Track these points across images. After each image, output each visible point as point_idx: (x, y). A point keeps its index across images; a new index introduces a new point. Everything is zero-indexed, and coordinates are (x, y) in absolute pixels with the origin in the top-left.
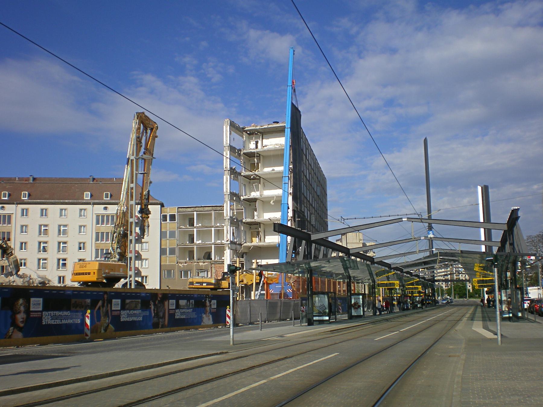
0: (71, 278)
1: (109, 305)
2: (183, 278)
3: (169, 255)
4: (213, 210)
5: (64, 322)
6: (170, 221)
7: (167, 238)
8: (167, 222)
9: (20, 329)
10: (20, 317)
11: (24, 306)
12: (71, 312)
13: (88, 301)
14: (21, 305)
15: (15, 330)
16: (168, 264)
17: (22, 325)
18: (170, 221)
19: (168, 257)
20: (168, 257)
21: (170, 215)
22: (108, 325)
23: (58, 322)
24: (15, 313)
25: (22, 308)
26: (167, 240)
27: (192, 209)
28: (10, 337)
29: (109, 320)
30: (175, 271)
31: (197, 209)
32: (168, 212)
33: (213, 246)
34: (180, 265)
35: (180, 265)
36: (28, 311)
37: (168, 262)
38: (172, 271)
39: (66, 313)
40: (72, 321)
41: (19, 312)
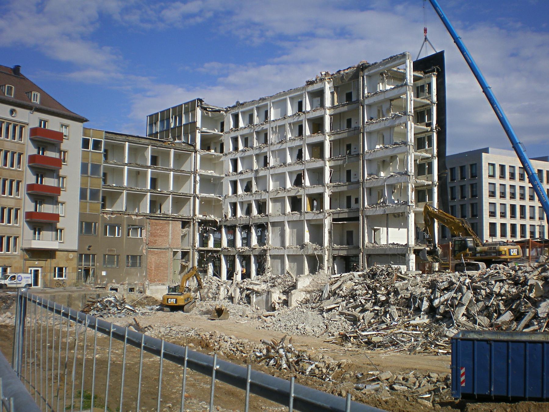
0: (58, 223)
2: (108, 236)
3: (91, 199)
4: (151, 144)
6: (93, 149)
7: (87, 174)
8: (89, 150)
16: (88, 212)
18: (93, 149)
19: (88, 204)
20: (88, 204)
21: (94, 140)
26: (88, 176)
27: (124, 137)
30: (98, 225)
31: (130, 138)
32: (91, 134)
33: (149, 194)
34: (105, 216)
35: (105, 216)
37: (88, 210)
38: (93, 223)
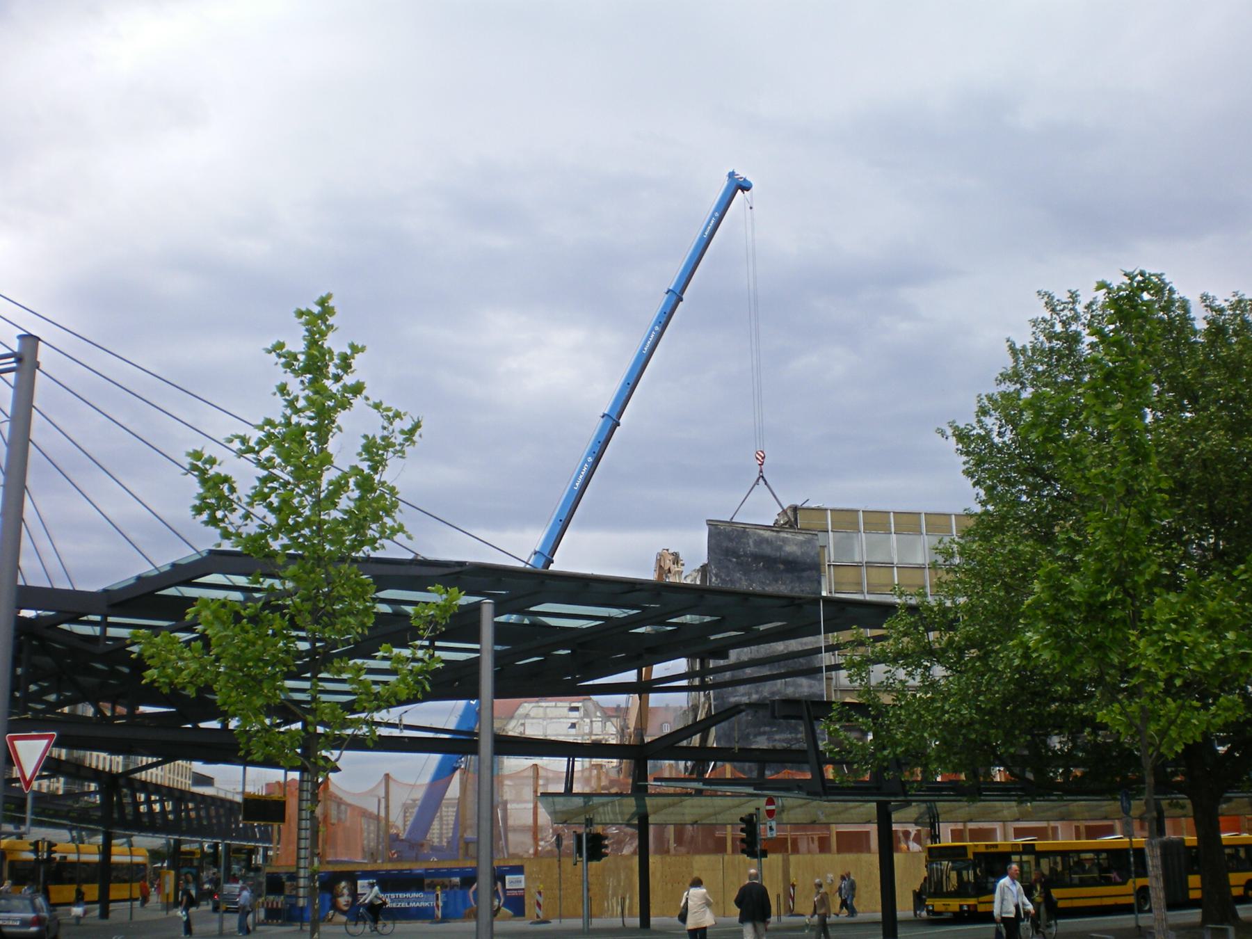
1: (499, 884)
5: (413, 905)
9: (344, 913)
10: (343, 901)
11: (349, 889)
12: (425, 893)
13: (457, 880)
14: (344, 888)
15: (337, 913)
17: (346, 908)
22: (499, 908)
23: (404, 905)
24: (335, 895)
25: (346, 891)
28: (330, 920)
29: (499, 902)
36: (354, 894)
39: (414, 895)
40: (427, 904)
41: (342, 895)
